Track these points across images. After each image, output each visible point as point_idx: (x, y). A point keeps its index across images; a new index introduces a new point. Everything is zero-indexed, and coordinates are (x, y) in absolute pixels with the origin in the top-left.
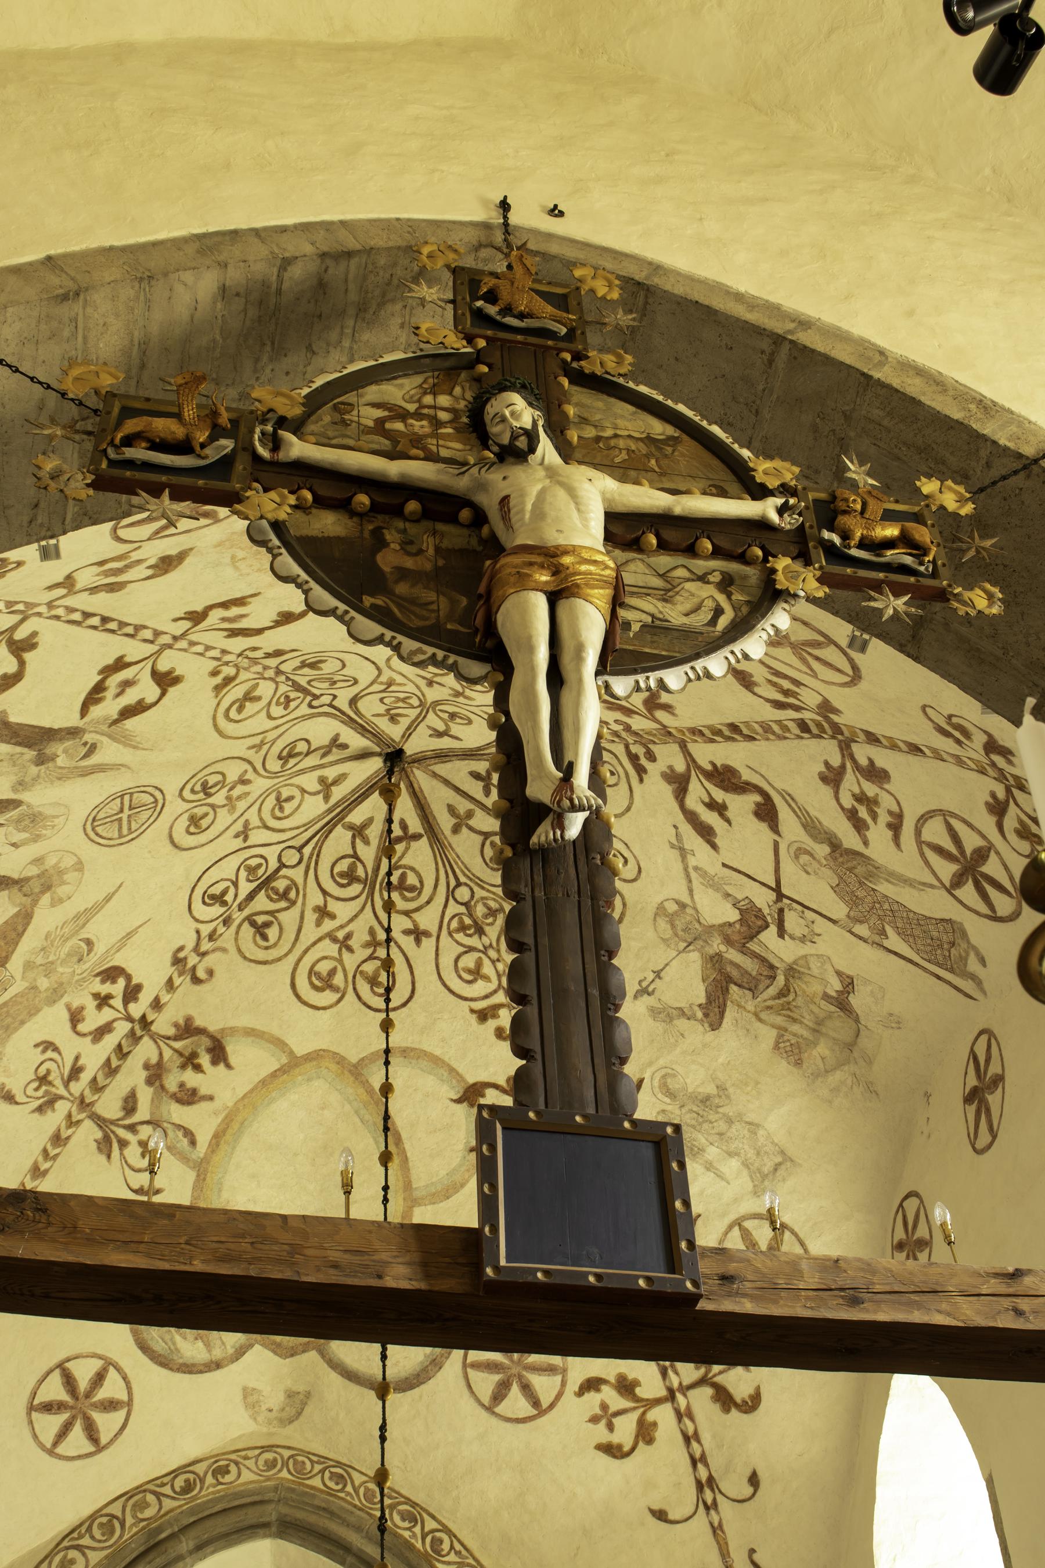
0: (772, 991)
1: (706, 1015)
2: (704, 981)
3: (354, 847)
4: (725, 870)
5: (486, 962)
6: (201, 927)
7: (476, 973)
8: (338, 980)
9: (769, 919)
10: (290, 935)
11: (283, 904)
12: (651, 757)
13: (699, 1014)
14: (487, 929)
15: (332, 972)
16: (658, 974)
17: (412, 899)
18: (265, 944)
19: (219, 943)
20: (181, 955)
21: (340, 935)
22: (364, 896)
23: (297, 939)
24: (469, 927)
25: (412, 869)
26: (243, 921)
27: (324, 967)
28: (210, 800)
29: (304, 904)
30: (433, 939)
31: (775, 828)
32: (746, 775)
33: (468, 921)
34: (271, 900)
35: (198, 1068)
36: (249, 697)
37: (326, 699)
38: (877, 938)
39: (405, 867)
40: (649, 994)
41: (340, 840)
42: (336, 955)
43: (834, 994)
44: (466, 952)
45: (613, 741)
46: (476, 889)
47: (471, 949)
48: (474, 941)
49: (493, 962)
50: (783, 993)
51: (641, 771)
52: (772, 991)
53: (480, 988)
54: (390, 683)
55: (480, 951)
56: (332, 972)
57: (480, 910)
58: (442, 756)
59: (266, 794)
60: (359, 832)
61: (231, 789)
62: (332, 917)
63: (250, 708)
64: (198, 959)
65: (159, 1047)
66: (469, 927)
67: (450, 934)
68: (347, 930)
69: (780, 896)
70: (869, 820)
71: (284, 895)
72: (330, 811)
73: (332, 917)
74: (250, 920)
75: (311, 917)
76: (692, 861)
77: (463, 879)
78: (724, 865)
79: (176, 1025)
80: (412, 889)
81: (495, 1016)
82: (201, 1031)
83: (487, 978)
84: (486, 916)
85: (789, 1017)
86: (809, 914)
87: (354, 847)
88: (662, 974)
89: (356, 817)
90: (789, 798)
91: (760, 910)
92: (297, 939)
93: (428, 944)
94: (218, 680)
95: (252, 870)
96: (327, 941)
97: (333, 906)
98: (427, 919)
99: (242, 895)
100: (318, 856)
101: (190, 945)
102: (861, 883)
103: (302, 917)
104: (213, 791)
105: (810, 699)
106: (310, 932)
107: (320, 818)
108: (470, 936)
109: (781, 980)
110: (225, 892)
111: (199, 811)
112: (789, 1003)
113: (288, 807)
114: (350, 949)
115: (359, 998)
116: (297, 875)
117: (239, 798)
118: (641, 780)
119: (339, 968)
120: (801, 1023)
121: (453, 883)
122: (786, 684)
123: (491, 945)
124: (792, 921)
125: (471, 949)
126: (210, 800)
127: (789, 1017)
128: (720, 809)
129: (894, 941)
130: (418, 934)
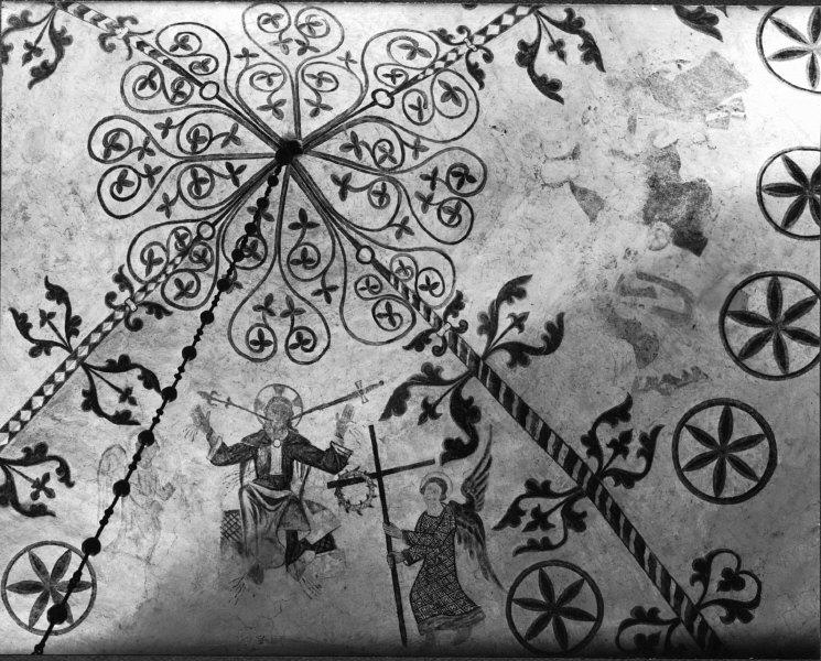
0: (267, 492)
1: (219, 452)
2: (244, 439)
3: (218, 136)
4: (367, 432)
5: (161, 267)
6: (154, 35)
7: (150, 262)
8: (115, 154)
9: (341, 473)
10: (144, 106)
11: (171, 94)
12: (438, 352)
13: (218, 447)
14: (187, 258)
15: (119, 148)
16: (229, 403)
17: (190, 192)
18: (137, 87)
19: (136, 52)
20: (128, 23)
21: (151, 145)
22: (183, 155)
23: (143, 112)
24: (182, 243)
25: (212, 187)
26: (154, 65)
27: (123, 140)
28: (293, 27)
29: (172, 110)
30: (165, 220)
31: (445, 459)
32: (480, 426)
33: (187, 241)
34: (173, 84)
35: (27, 59)
36: (414, 51)
37: (383, 99)
38: (398, 557)
39: (213, 180)
40: (209, 402)
41: (222, 123)
42: (135, 146)
43: (300, 537)
44: (164, 248)
45: (428, 320)
46: (214, 240)
47: (166, 250)
48: (173, 253)
49: (164, 271)
50: (270, 500)
51: (419, 344)
52: (267, 492)
53: (140, 268)
54: (417, 149)
55: (168, 258)
56: (119, 148)
57: (198, 248)
58: (308, 185)
59: (283, 67)
60: (231, 137)
61: (298, 42)
62: (165, 135)
63: (401, 56)
64: (121, 36)
65: (44, 19)
66: (182, 243)
67: (175, 231)
68: (155, 149)
69: (379, 474)
70: (523, 526)
71: (178, 93)
72: (249, 111)
73: (165, 135)
74: (156, 70)
75: (162, 119)
76: (356, 403)
77: (217, 227)
78: (371, 428)
79: (64, 30)
80: (198, 190)
81: (122, 288)
82: (60, 55)
83: (148, 271)
84: (196, 254)
85: (255, 511)
86: (377, 502)
87: (218, 136)
88: (230, 406)
89: (242, 132)
90: (487, 462)
91: (346, 463)
92: (143, 112)
93: (162, 217)
94: (452, 30)
95: (204, 65)
96: (145, 135)
97: (172, 133)
98: (180, 211)
99: (176, 60)
100: (210, 111)
101: (135, 28)
102: (452, 533)
103: (161, 112)
104: (305, 30)
105: (632, 463)
106: (149, 122)
107: (243, 105)
108: (176, 247)
109: (281, 494)
110: (185, 47)
111: (283, 23)
112: (265, 507)
113: (263, 84)
114: (140, 157)
115: (105, 174)
116: (196, 99)
117: (286, 47)
118: (407, 348)
119: (123, 153)
120: (256, 523)
121: (211, 220)
122: (635, 445)
123: (176, 266)
124: (354, 493)
125: (166, 250)
126: (293, 27)
127: (255, 511)
128: (429, 411)
129: (409, 575)
130: (166, 207)
